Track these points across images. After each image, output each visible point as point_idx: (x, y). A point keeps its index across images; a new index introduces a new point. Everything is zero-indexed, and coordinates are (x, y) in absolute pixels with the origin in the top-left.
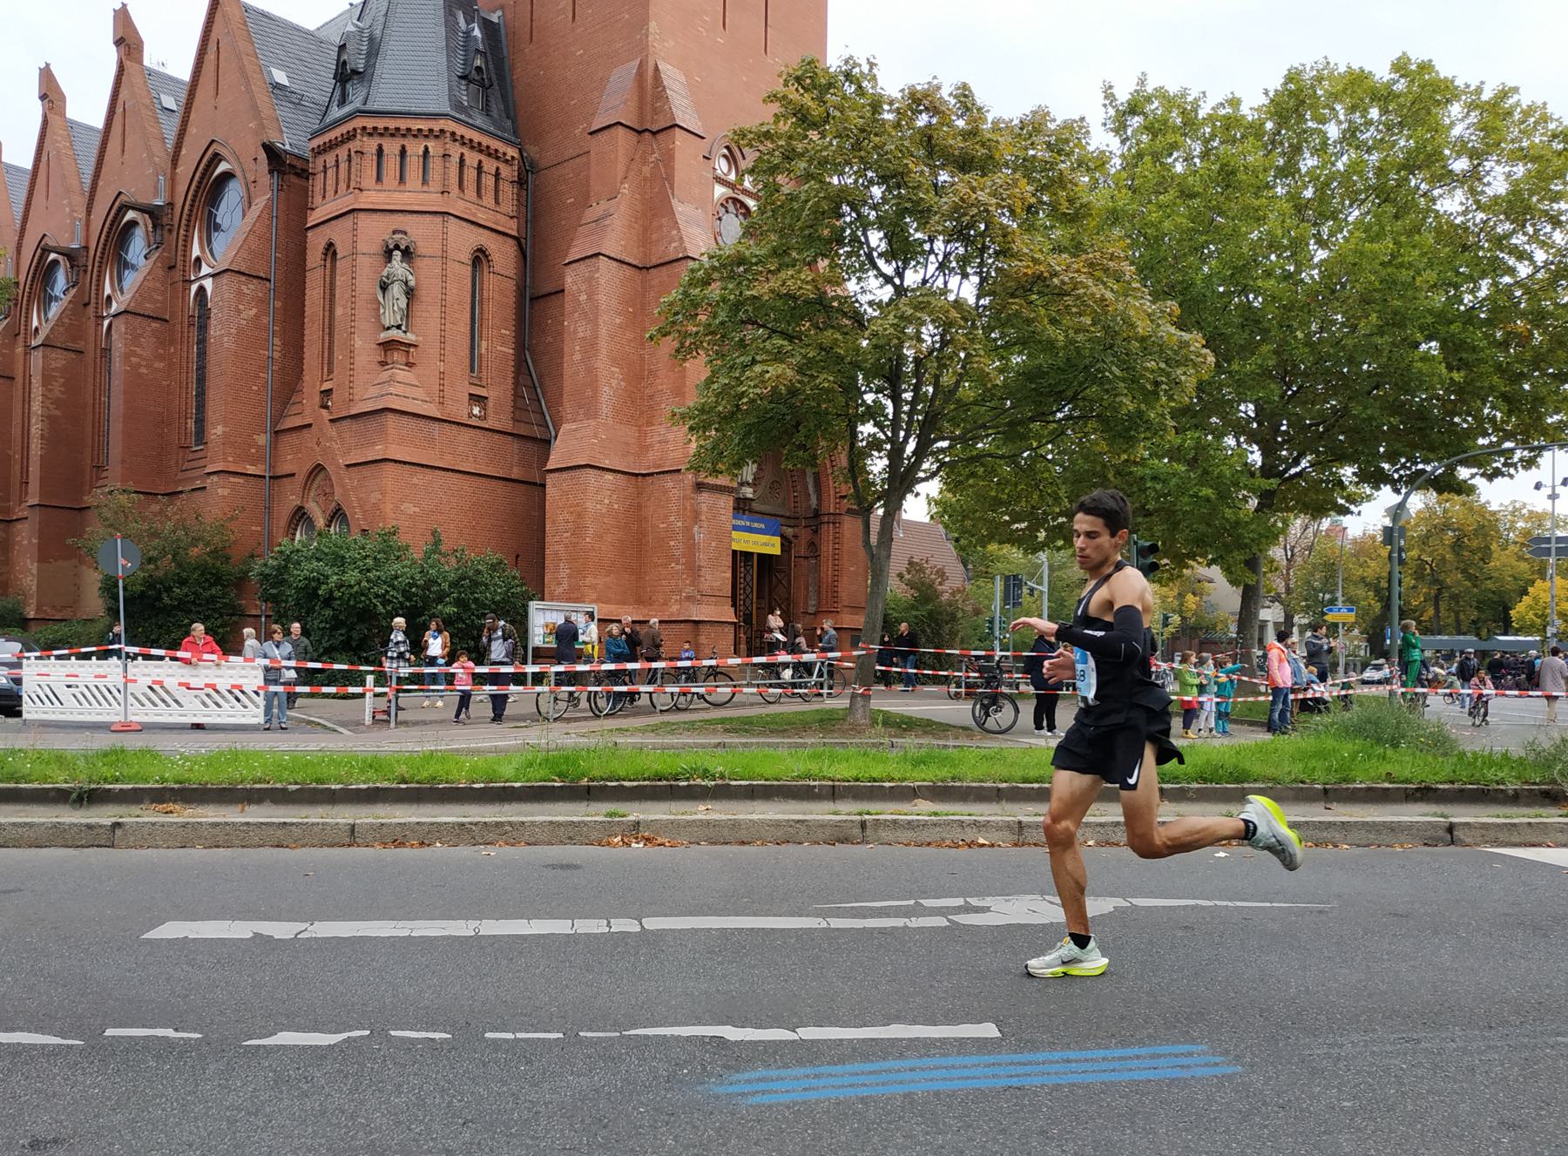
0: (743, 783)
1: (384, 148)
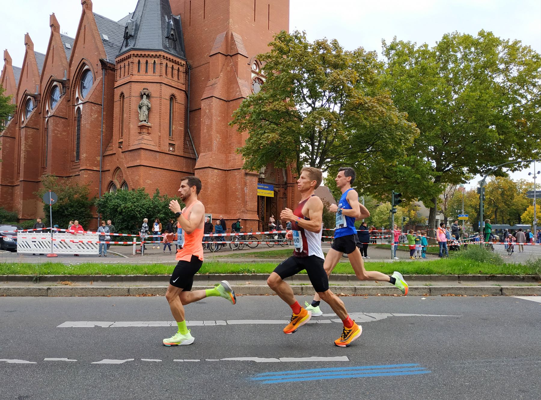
0: (261, 274)
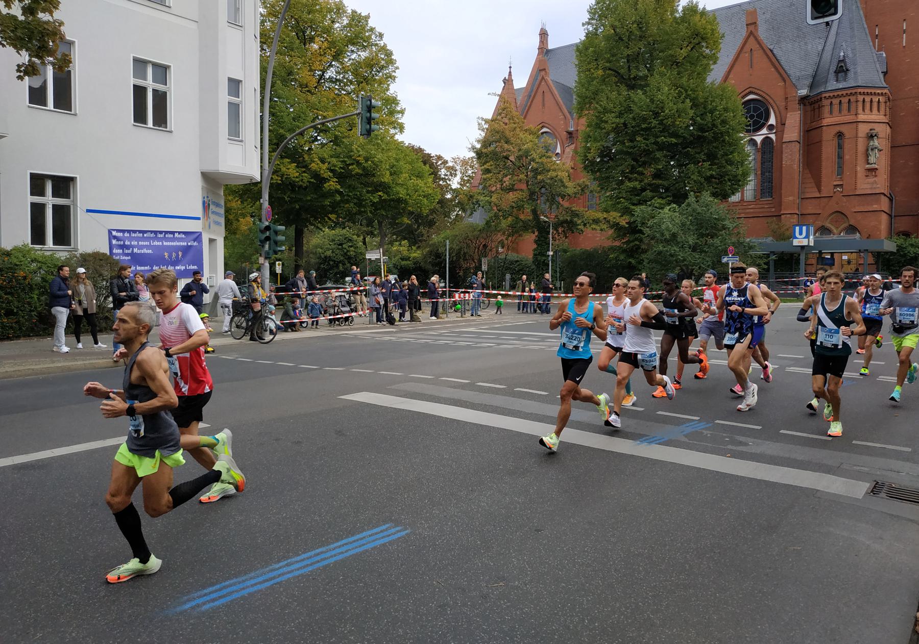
1: (866, 99)
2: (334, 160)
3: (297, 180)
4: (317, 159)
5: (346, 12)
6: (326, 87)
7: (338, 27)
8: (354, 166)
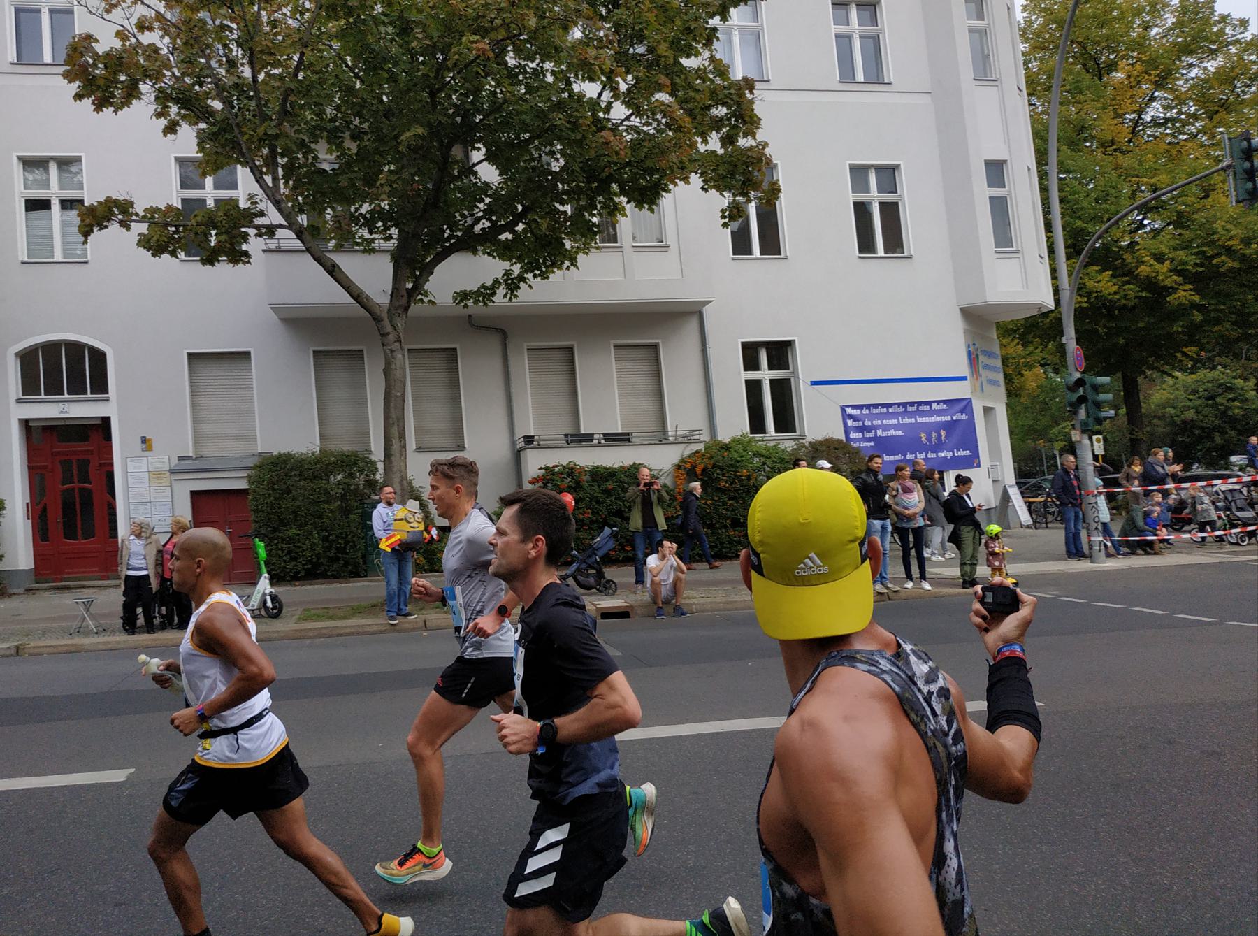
2: (1181, 255)
3: (1117, 297)
4: (1149, 258)
5: (1169, 6)
6: (1149, 136)
7: (1157, 34)
8: (1224, 257)
